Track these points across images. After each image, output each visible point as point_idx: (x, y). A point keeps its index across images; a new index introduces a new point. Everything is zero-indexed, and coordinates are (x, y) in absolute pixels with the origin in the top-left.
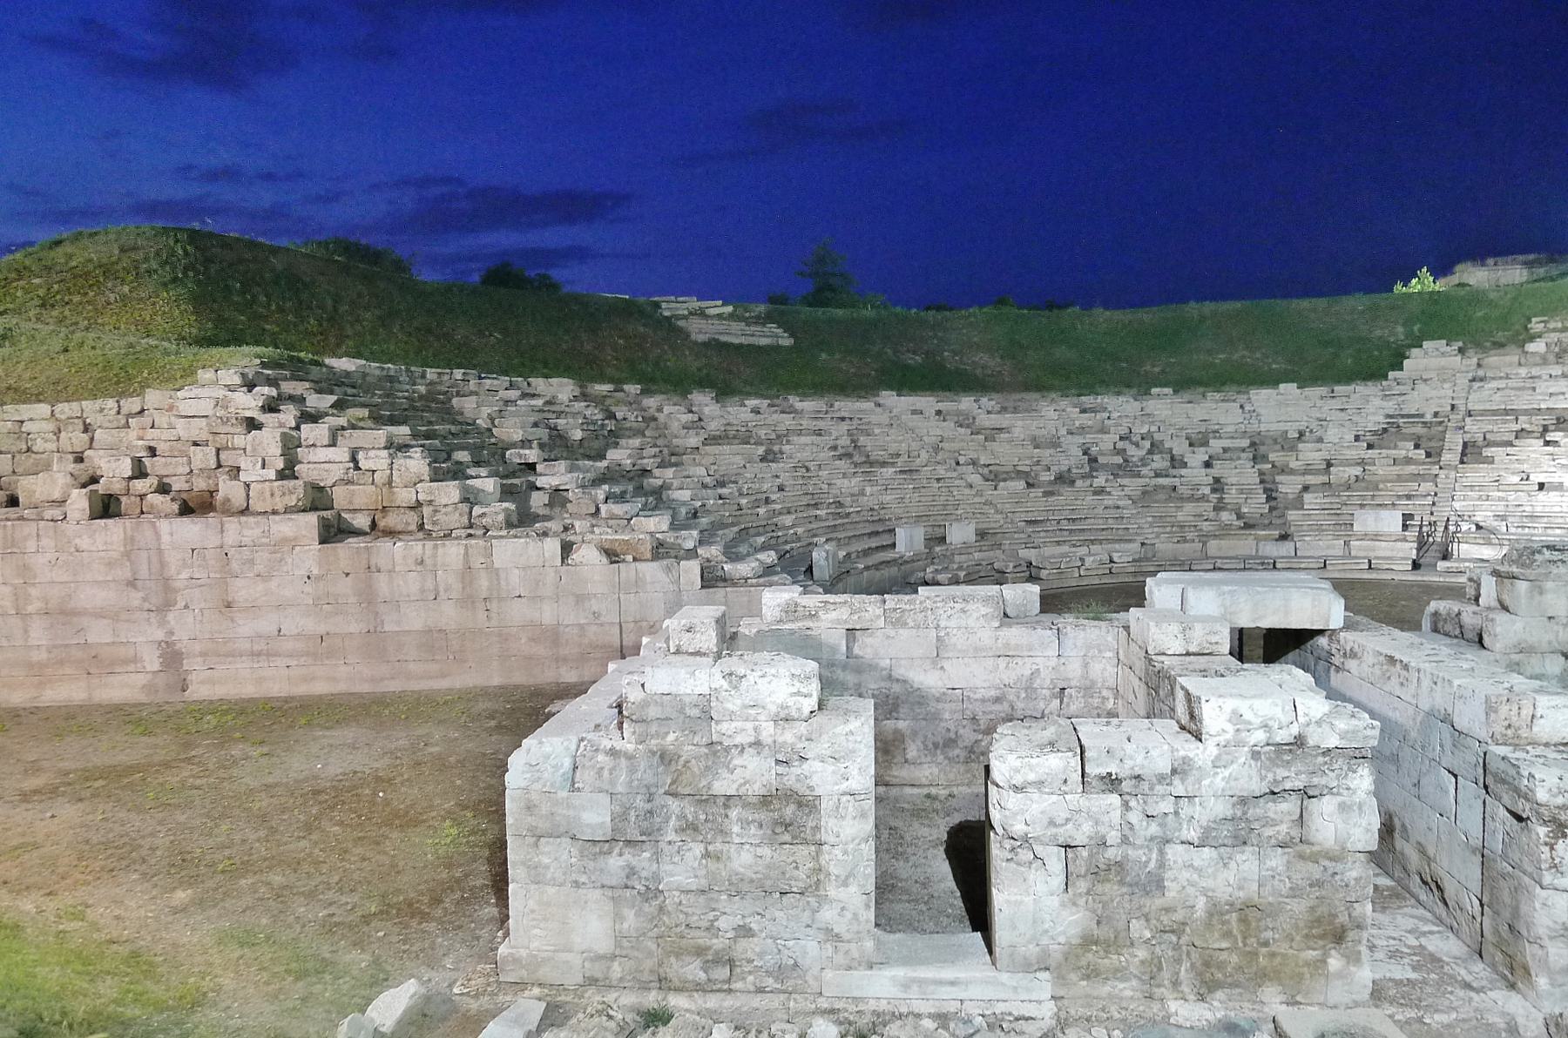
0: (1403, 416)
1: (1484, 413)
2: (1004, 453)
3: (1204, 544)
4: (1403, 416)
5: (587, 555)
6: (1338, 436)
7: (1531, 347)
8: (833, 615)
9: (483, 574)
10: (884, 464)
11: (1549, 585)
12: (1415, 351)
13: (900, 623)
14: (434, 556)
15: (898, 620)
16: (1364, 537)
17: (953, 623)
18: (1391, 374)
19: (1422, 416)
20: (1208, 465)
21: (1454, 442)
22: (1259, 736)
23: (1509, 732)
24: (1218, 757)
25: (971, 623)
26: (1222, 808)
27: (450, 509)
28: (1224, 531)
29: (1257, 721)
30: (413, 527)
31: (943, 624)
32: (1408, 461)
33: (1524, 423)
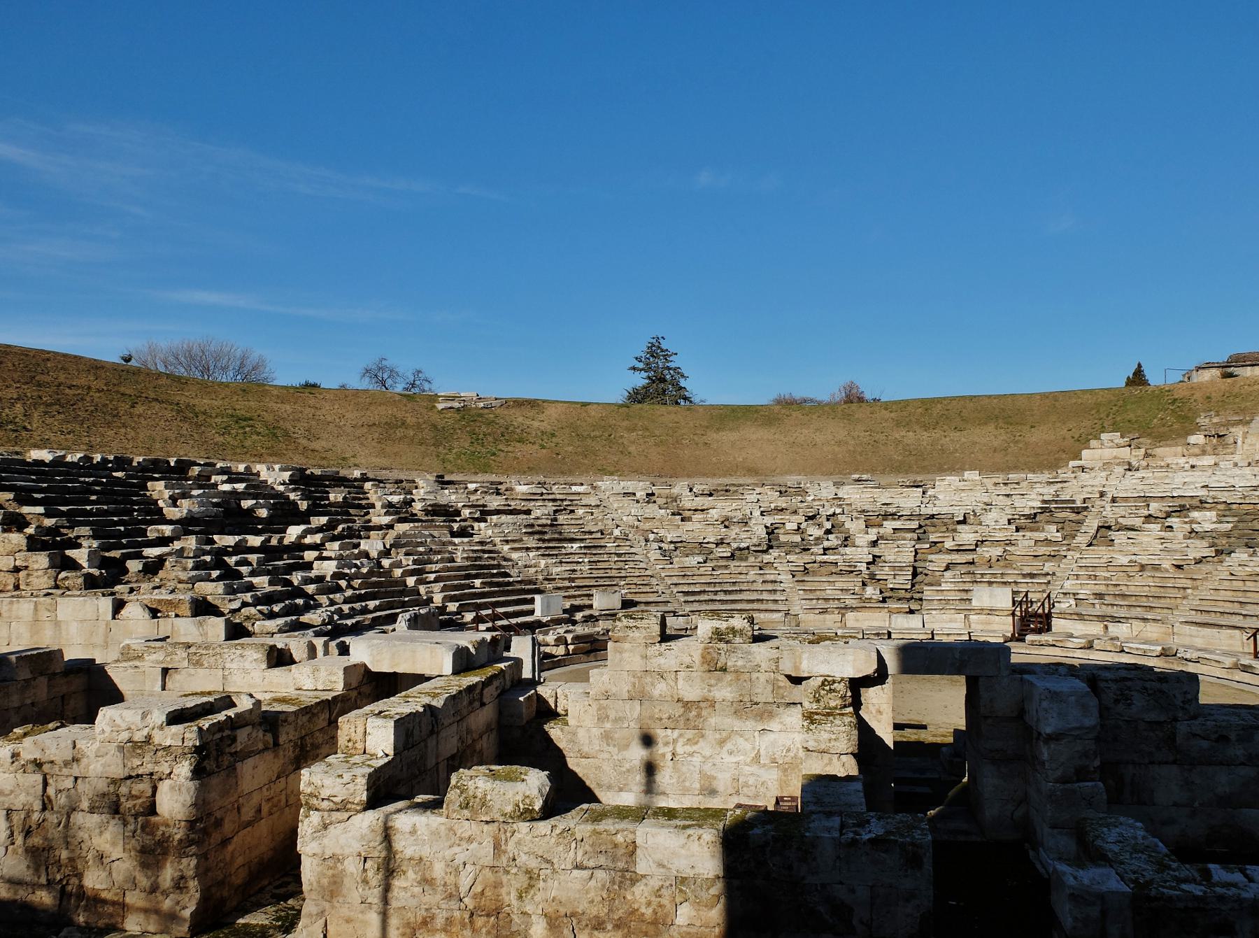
0: (1056, 502)
1: (1126, 499)
2: (695, 529)
3: (843, 615)
4: (1056, 502)
5: (133, 611)
6: (995, 521)
7: (1192, 439)
8: (154, 657)
9: (48, 625)
10: (572, 540)
11: (627, 646)
12: (1093, 443)
13: (198, 664)
14: (10, 610)
15: (198, 662)
16: (981, 611)
17: (234, 666)
18: (1072, 463)
19: (1073, 502)
20: (874, 544)
21: (1092, 524)
22: (125, 736)
23: (350, 744)
24: (98, 750)
25: (247, 665)
26: (102, 786)
27: (40, 573)
28: (864, 605)
29: (124, 726)
30: (11, 587)
31: (228, 665)
32: (1047, 542)
33: (1155, 508)
